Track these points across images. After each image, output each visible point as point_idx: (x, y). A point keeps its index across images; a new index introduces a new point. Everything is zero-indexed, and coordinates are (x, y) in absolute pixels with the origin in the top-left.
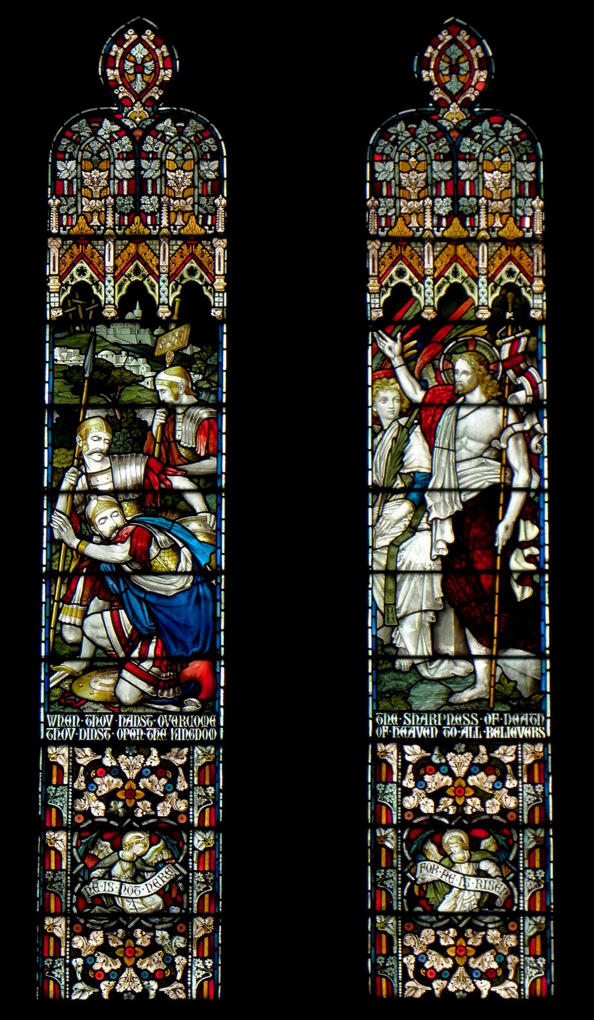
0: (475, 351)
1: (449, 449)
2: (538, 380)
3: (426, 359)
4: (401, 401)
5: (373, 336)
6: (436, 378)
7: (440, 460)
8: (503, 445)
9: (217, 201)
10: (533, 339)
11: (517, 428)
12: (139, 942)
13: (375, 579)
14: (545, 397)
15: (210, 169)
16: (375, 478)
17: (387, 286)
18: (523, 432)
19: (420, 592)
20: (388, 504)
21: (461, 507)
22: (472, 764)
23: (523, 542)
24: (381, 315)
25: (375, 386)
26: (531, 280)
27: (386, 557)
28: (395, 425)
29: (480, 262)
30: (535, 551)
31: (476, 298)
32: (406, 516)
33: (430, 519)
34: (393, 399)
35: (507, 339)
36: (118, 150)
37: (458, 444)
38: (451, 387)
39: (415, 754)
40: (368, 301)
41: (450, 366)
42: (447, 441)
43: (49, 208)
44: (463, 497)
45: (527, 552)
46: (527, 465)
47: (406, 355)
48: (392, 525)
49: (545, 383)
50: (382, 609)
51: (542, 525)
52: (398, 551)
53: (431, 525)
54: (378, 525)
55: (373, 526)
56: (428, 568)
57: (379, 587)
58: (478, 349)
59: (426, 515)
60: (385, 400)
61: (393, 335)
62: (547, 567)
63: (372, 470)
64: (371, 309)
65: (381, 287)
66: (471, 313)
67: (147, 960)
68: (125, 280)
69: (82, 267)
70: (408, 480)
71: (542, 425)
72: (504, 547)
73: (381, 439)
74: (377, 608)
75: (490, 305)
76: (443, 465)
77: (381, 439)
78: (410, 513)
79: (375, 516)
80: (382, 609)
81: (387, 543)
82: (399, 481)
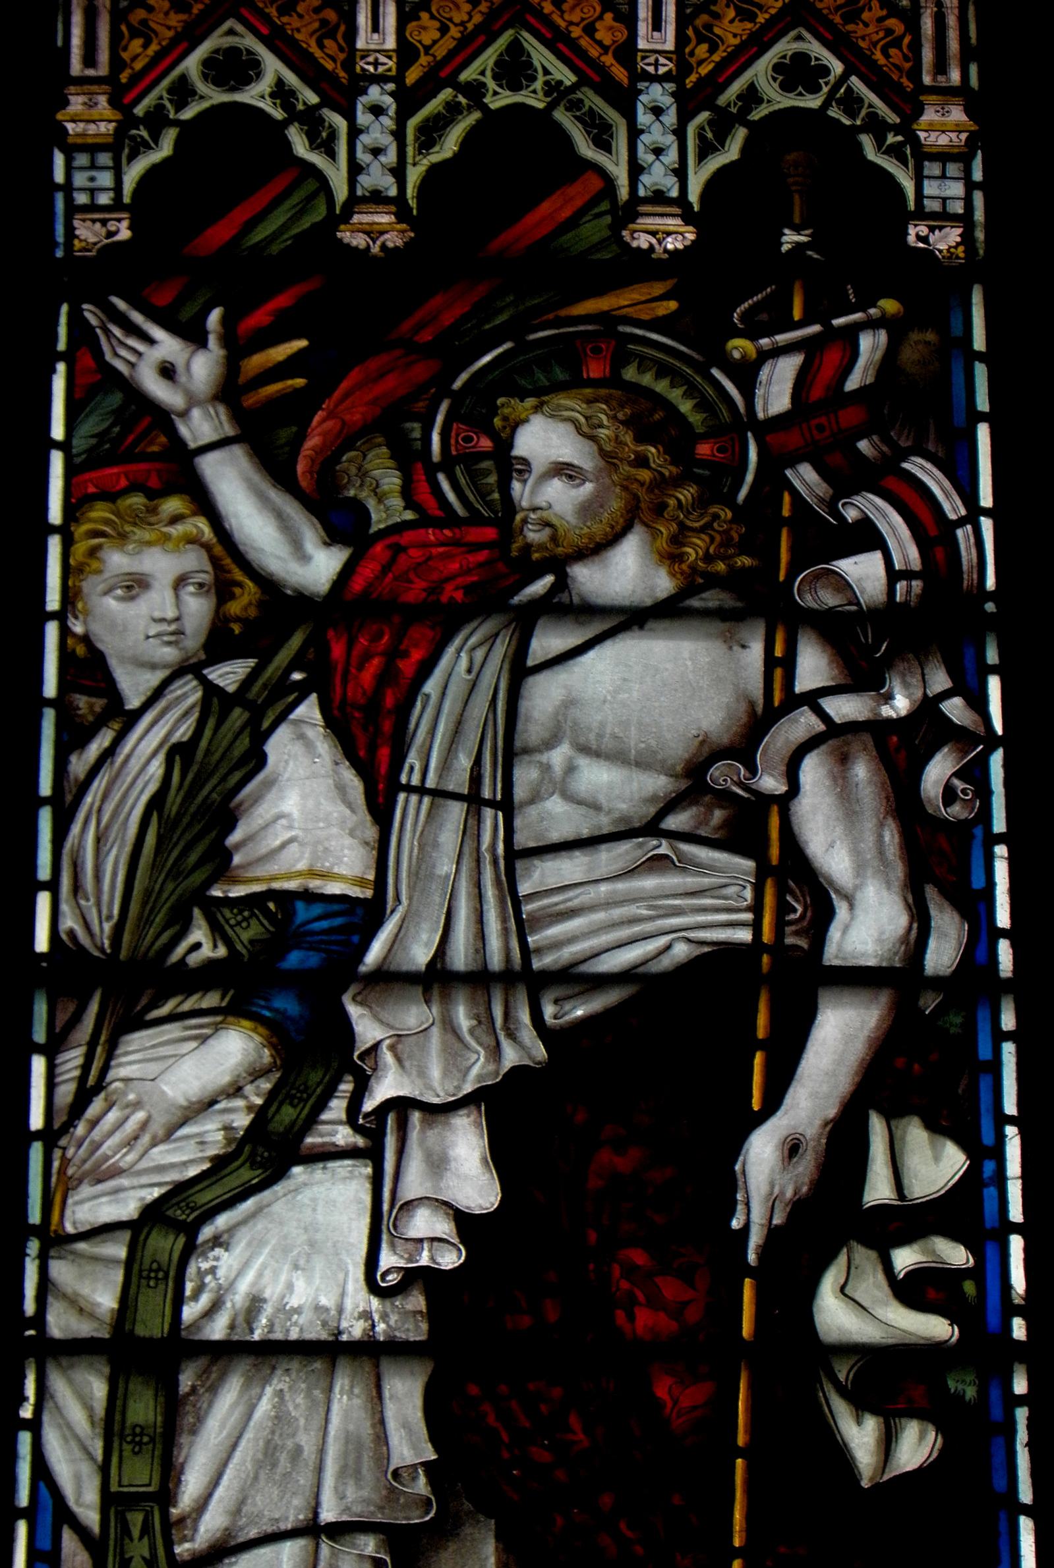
0: (614, 380)
1: (474, 800)
2: (953, 507)
3: (356, 416)
4: (222, 589)
5: (77, 322)
6: (407, 493)
7: (426, 845)
8: (771, 783)
10: (920, 341)
11: (844, 708)
13: (58, 1384)
14: (991, 583)
16: (69, 922)
17: (157, 121)
18: (877, 729)
19: (307, 1441)
20: (137, 1040)
21: (540, 1052)
23: (881, 1209)
24: (125, 234)
25: (80, 530)
26: (910, 109)
27: (119, 1276)
28: (189, 692)
29: (643, 28)
30: (957, 1255)
31: (620, 173)
32: (235, 1090)
33: (369, 1106)
34: (180, 582)
35: (782, 338)
37: (525, 776)
38: (490, 533)
40: (59, 176)
41: (486, 443)
42: (464, 762)
44: (549, 1010)
45: (905, 1258)
46: (899, 871)
47: (250, 400)
48: (157, 1127)
49: (987, 524)
50: (91, 1517)
51: (988, 1139)
52: (190, 1250)
53: (375, 1136)
54: (80, 1129)
55: (51, 1136)
56: (356, 1330)
57: (77, 1415)
58: (630, 373)
59: (346, 1087)
60: (136, 585)
61: (188, 312)
62: (1019, 1329)
63: (53, 886)
64: (72, 209)
65: (127, 122)
66: (594, 230)
70: (249, 932)
71: (979, 703)
72: (773, 1234)
73: (108, 754)
74: (64, 1515)
75: (694, 196)
76: (446, 867)
77: (108, 754)
78: (256, 1074)
79: (66, 1092)
80: (91, 1517)
81: (128, 1209)
82: (199, 933)
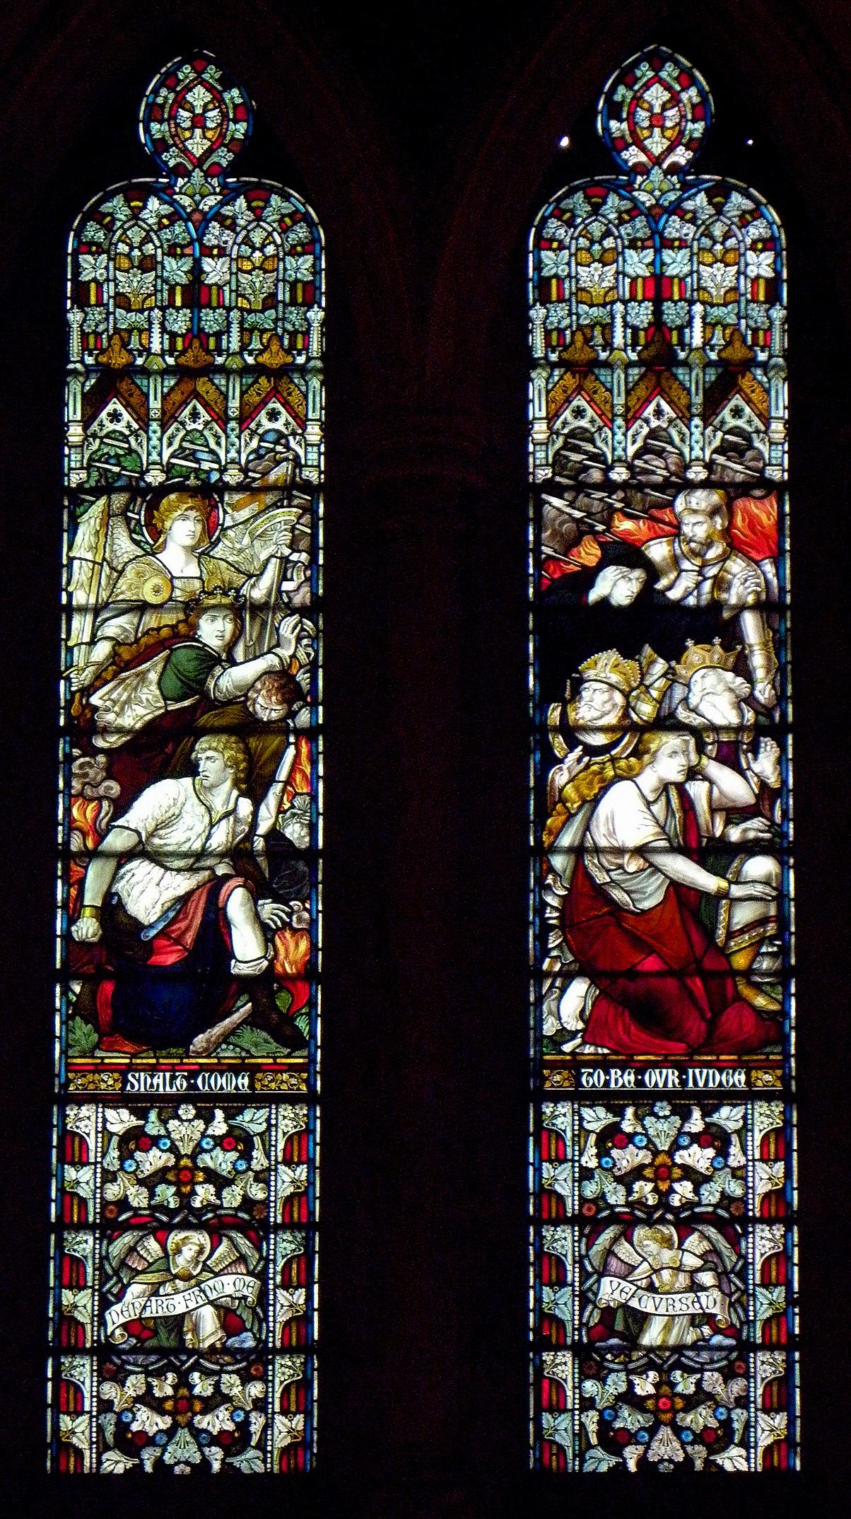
15: (302, 267)
22: (680, 1133)
39: (599, 1119)
43: (67, 324)
67: (208, 1418)
68: (178, 430)
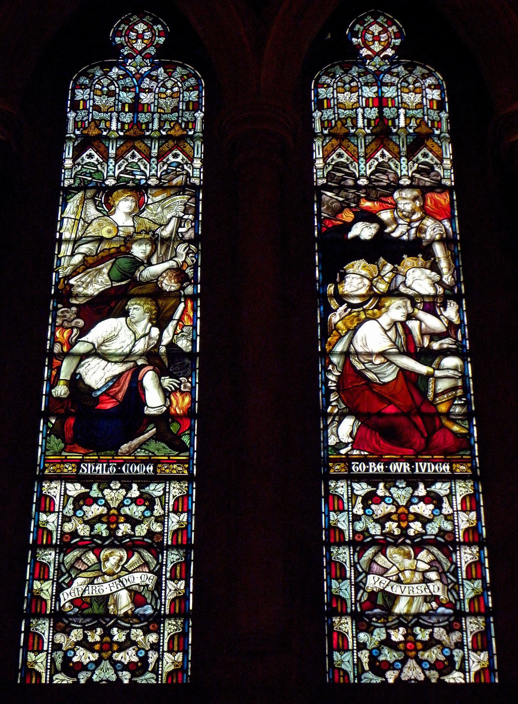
9: (196, 114)
12: (115, 639)
22: (412, 496)
36: (122, 85)
39: (363, 489)
43: (68, 118)
67: (122, 654)
68: (124, 162)
69: (90, 154)
